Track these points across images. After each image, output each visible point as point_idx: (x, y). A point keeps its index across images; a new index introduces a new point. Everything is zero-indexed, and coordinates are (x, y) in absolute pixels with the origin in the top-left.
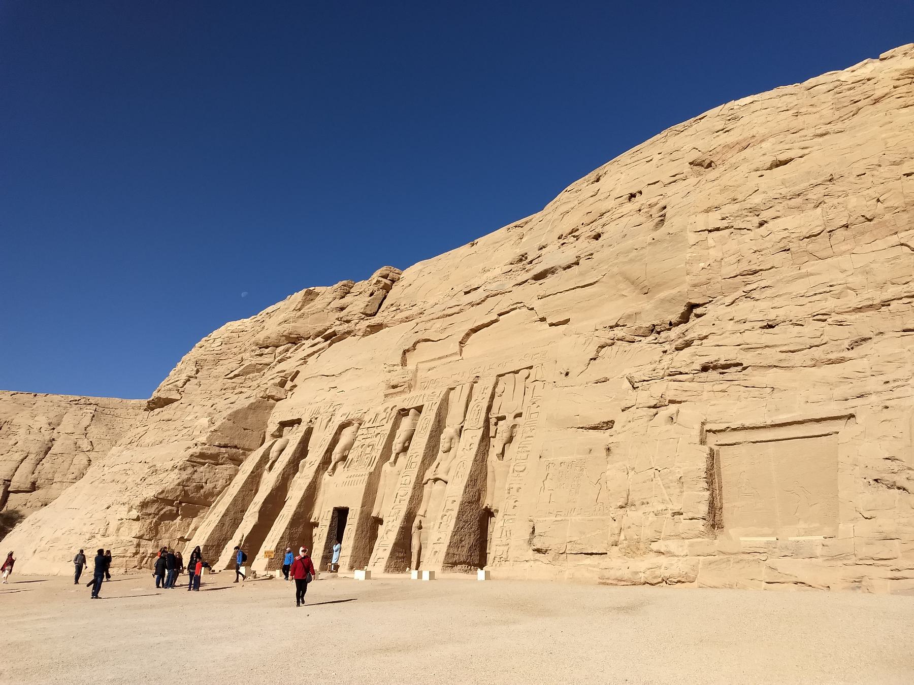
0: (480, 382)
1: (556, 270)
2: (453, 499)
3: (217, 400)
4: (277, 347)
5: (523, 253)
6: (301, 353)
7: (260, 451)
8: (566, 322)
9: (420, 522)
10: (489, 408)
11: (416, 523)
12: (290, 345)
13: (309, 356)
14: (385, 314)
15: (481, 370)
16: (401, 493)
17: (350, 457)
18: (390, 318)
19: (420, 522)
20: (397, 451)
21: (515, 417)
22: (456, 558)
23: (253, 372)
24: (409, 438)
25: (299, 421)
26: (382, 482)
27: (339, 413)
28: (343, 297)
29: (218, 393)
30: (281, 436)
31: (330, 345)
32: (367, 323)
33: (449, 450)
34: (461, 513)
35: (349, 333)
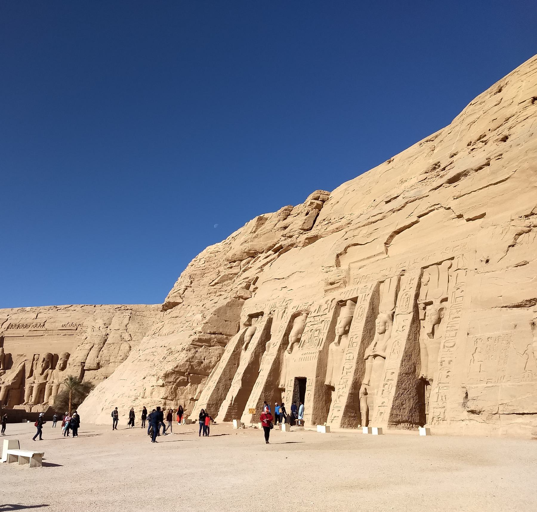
1: (468, 172)
2: (392, 371)
3: (206, 301)
4: (241, 261)
5: (436, 162)
6: (258, 264)
7: (237, 336)
8: (483, 216)
9: (366, 389)
10: (417, 296)
11: (362, 390)
13: (264, 265)
14: (319, 227)
16: (347, 366)
18: (323, 230)
19: (366, 389)
20: (340, 334)
21: (442, 302)
22: (399, 418)
23: (227, 280)
24: (349, 323)
25: (262, 314)
26: (330, 358)
27: (290, 306)
29: (206, 296)
30: (250, 325)
31: (279, 256)
32: (305, 236)
33: (384, 332)
34: (400, 382)
35: (292, 245)
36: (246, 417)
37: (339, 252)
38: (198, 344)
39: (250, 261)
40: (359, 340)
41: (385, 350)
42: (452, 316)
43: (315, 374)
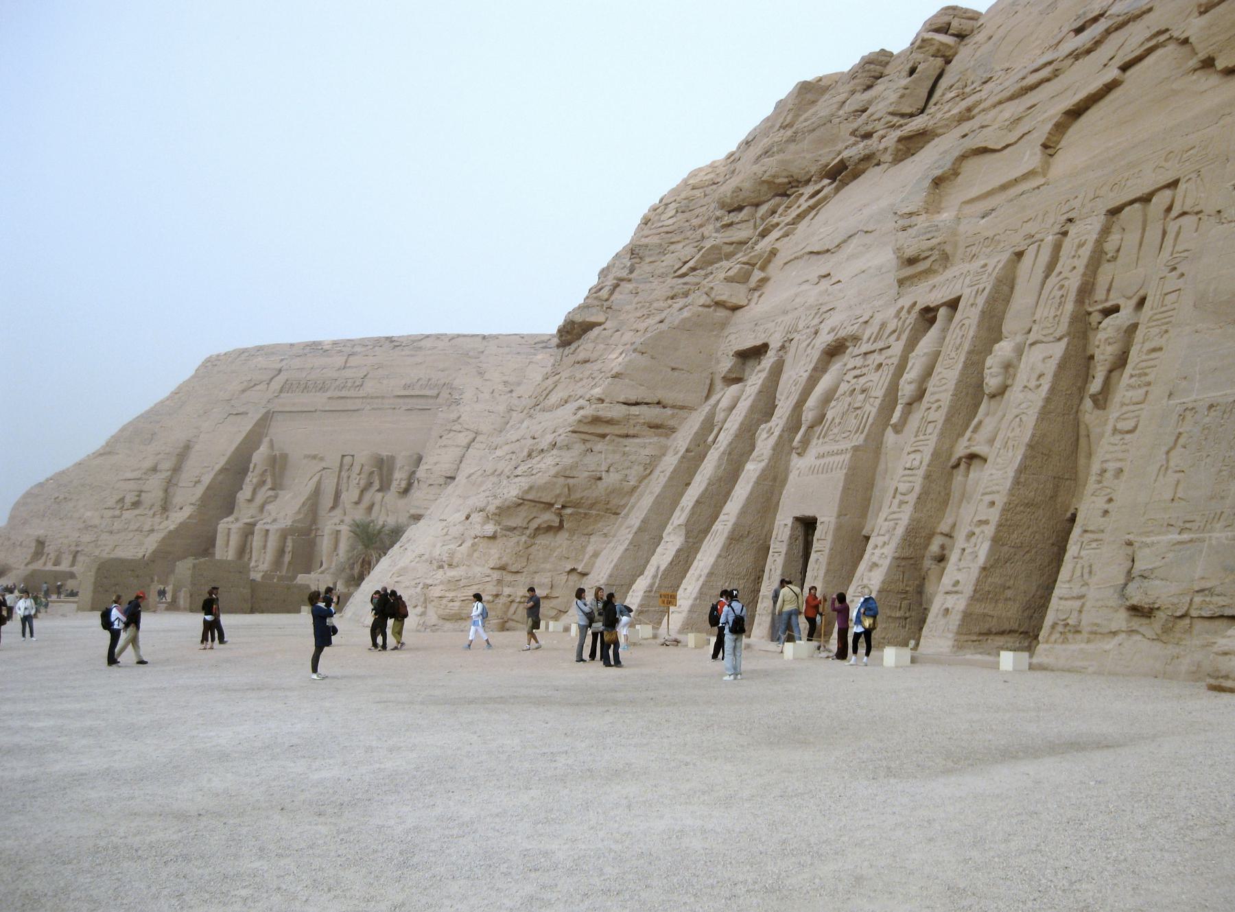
0: (1073, 230)
6: (794, 213)
9: (943, 547)
11: (934, 548)
12: (778, 199)
15: (1076, 203)
16: (903, 487)
17: (829, 415)
24: (928, 373)
27: (825, 328)
28: (869, 87)
29: (662, 304)
30: (738, 380)
31: (837, 190)
32: (898, 133)
36: (677, 617)
37: (938, 172)
38: (592, 429)
39: (779, 205)
40: (939, 416)
41: (991, 441)
42: (1148, 346)
43: (836, 509)
